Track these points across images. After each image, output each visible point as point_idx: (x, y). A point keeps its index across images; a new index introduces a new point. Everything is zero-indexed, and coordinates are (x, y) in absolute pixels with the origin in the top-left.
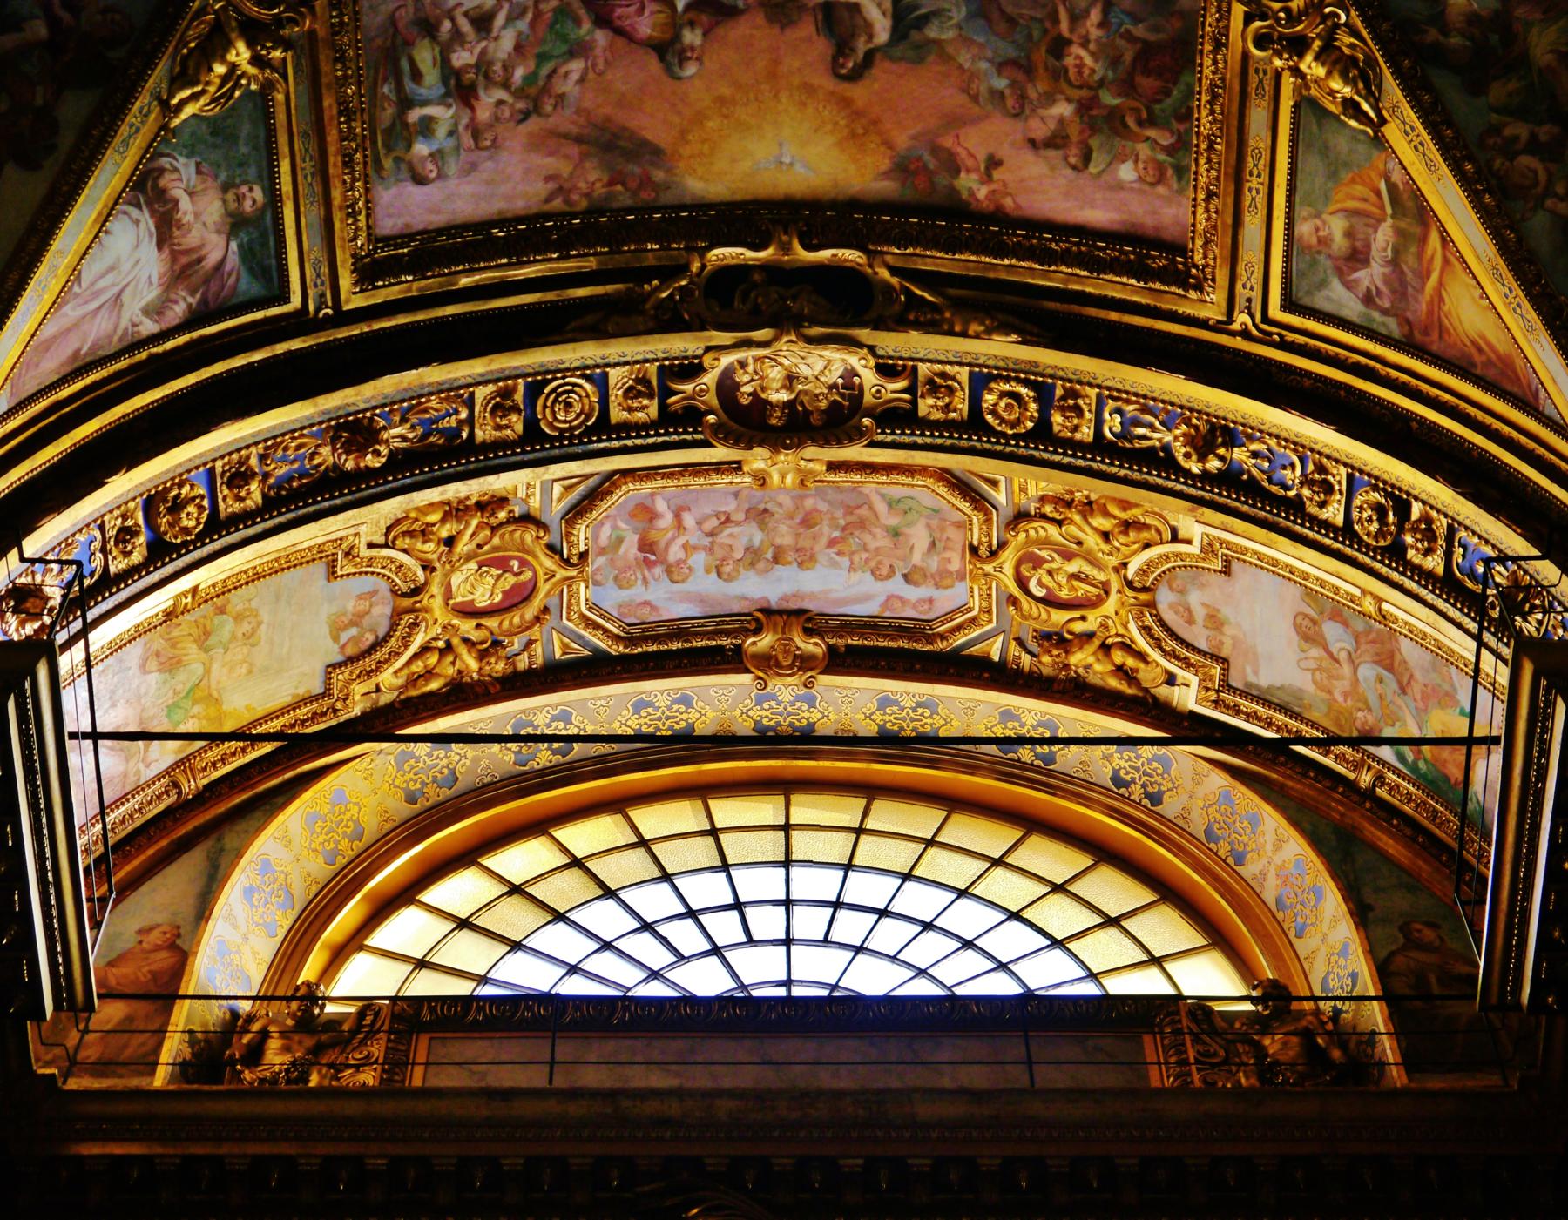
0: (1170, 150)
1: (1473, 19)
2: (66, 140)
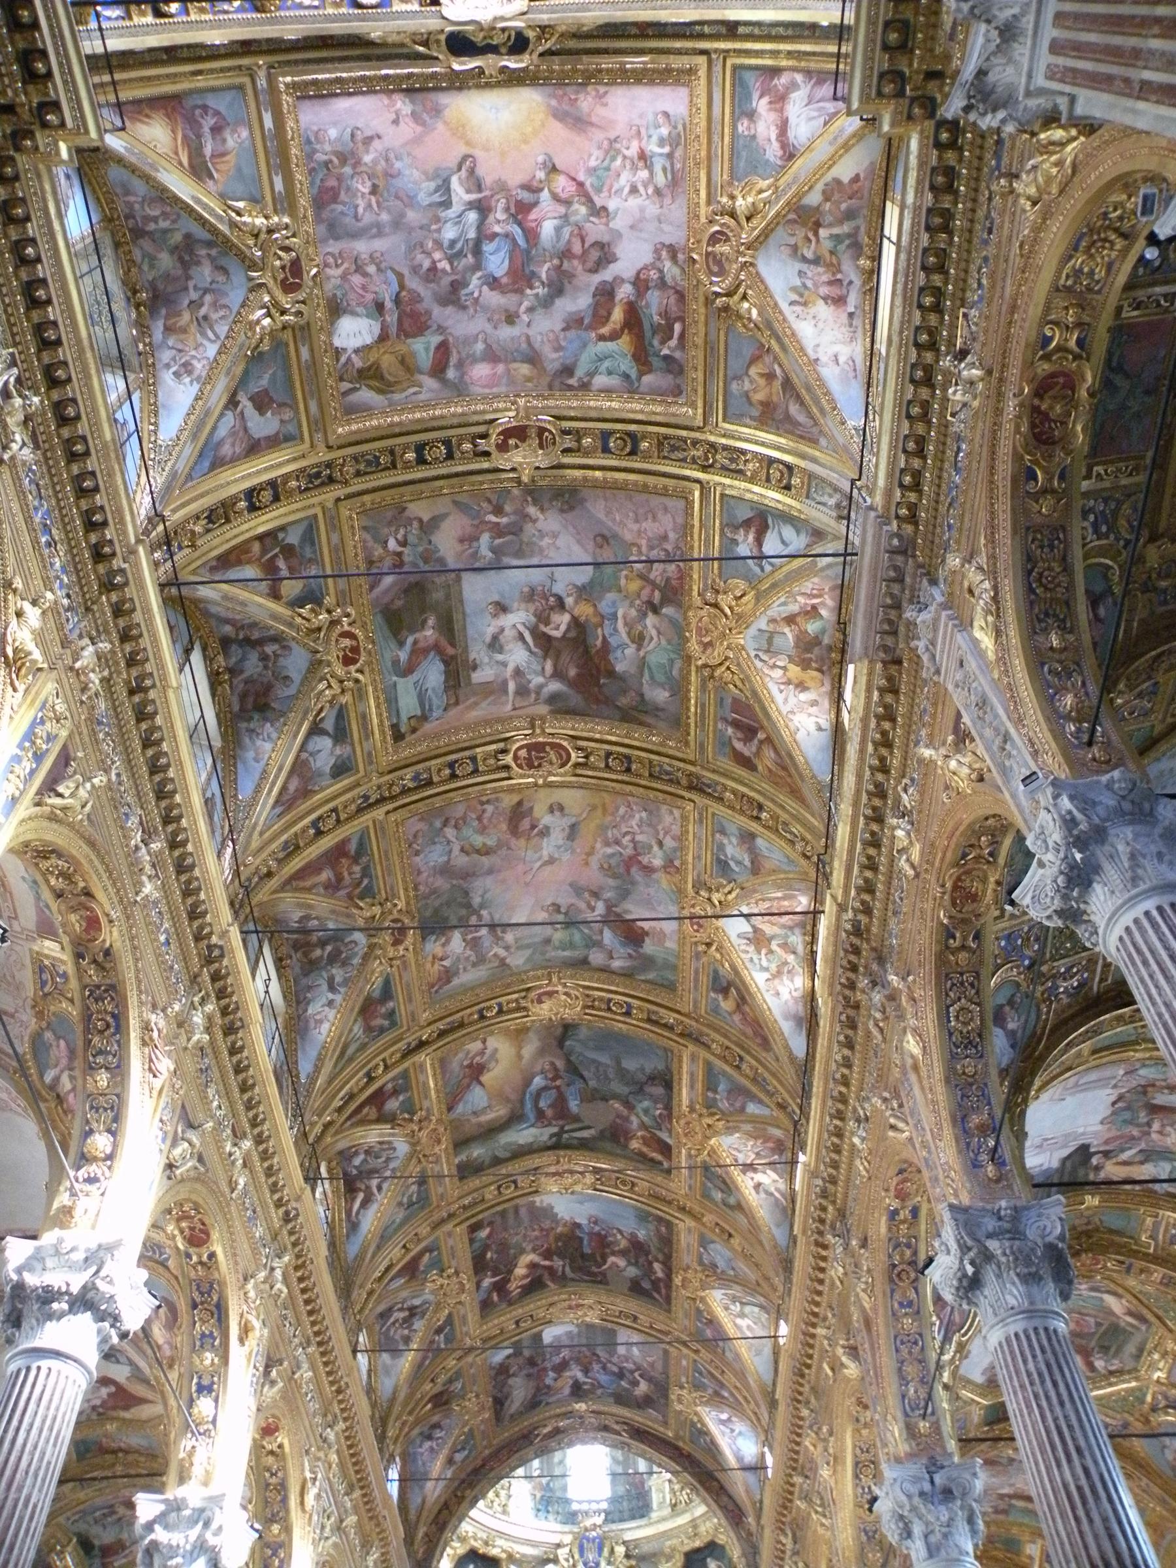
0: (314, 151)
1: (198, 263)
2: (820, 187)
